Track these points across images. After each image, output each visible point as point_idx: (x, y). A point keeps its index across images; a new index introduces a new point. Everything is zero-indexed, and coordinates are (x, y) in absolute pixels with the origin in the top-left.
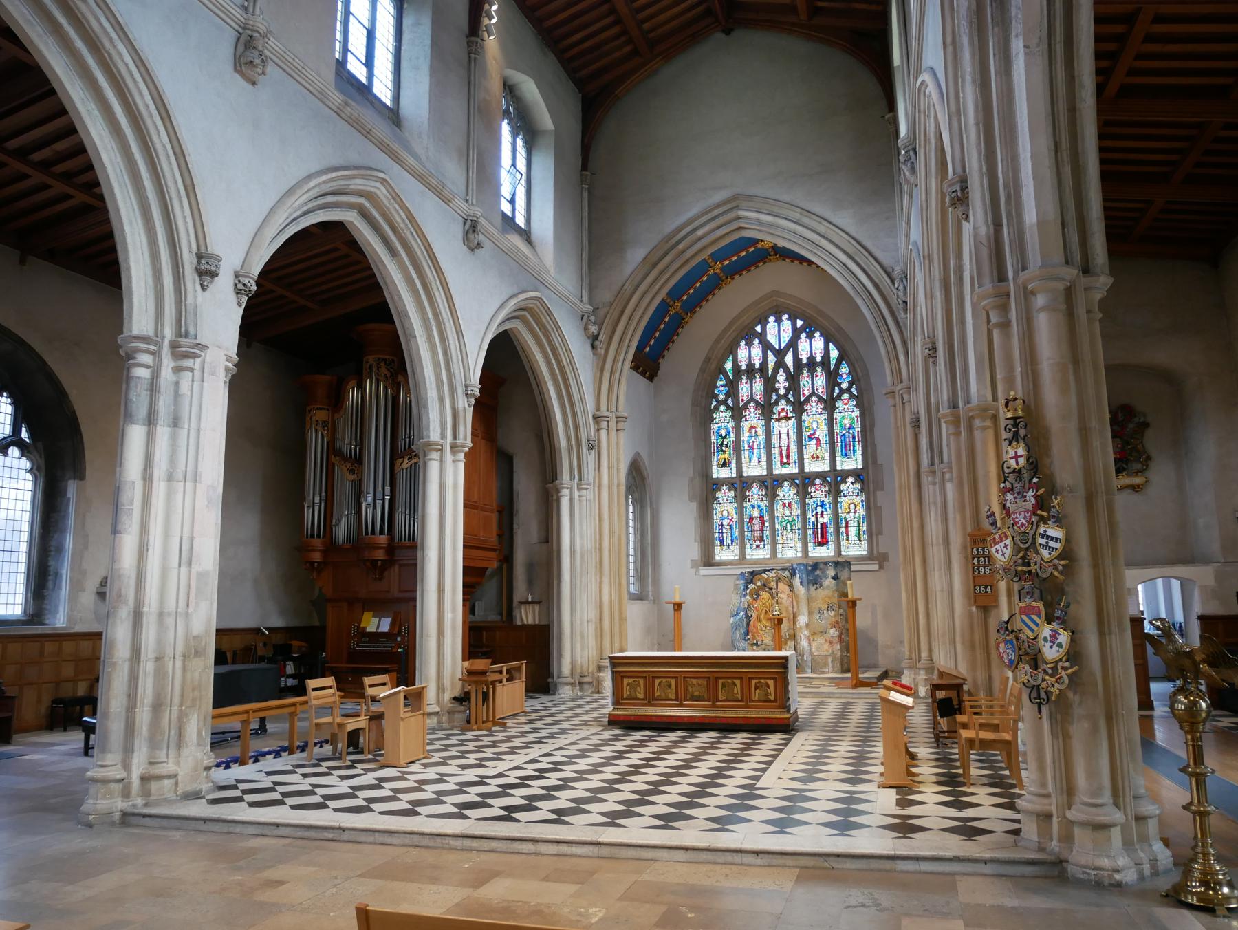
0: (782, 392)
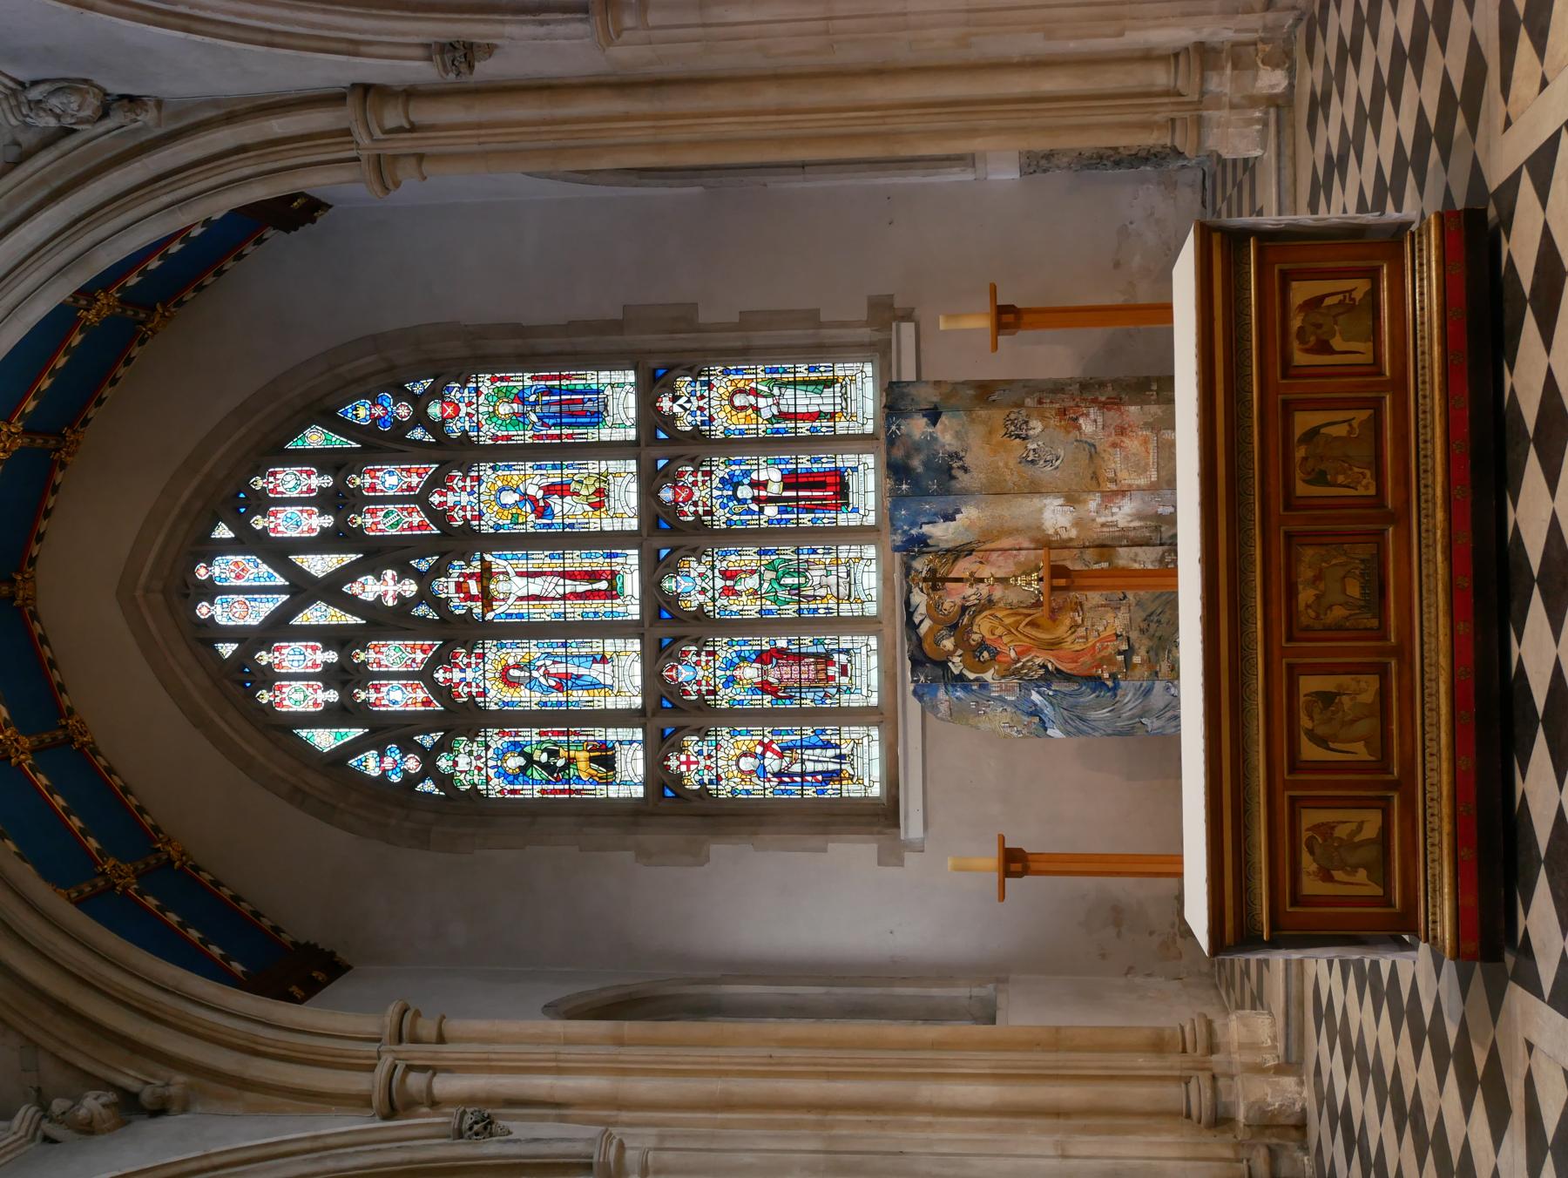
0: (410, 588)
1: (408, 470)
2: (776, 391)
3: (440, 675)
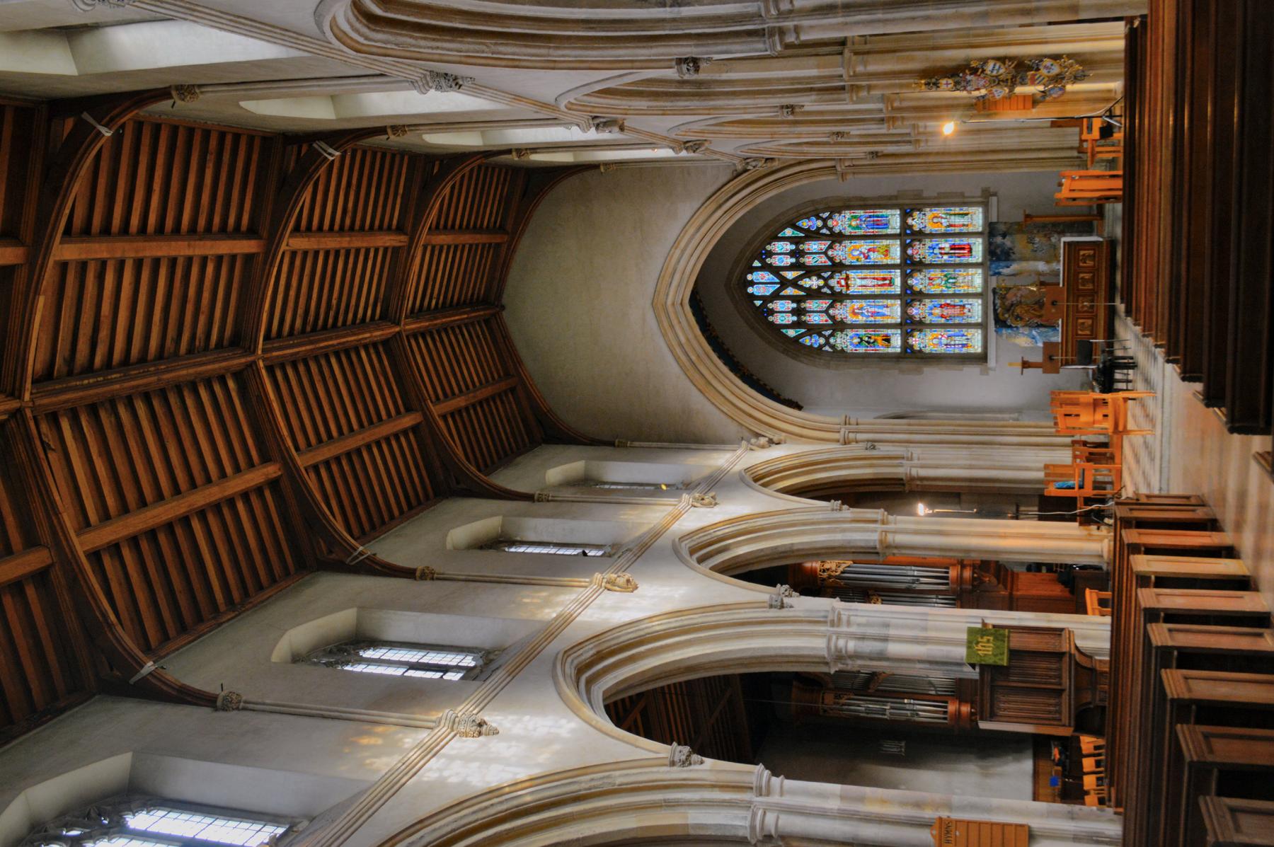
0: (821, 283)
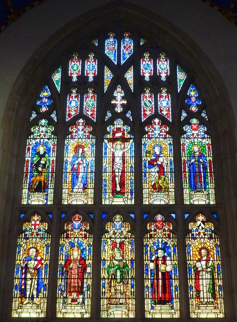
0: (119, 110)
1: (169, 110)
2: (209, 270)
3: (81, 121)
